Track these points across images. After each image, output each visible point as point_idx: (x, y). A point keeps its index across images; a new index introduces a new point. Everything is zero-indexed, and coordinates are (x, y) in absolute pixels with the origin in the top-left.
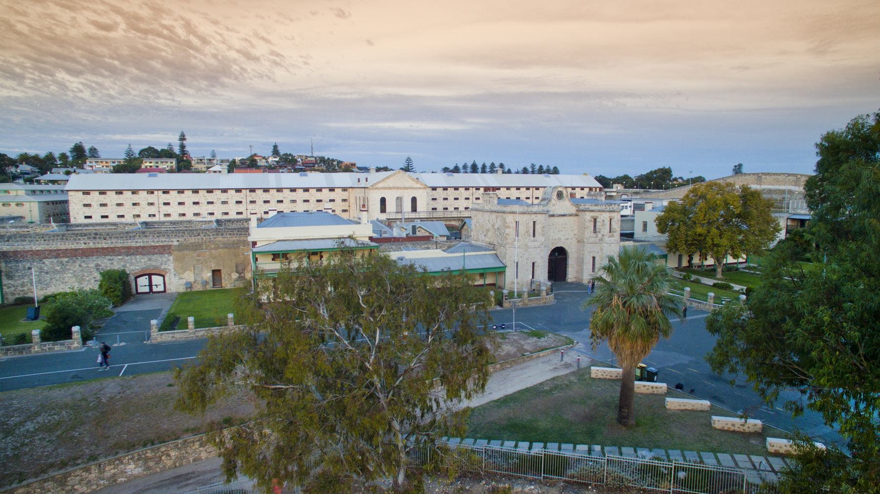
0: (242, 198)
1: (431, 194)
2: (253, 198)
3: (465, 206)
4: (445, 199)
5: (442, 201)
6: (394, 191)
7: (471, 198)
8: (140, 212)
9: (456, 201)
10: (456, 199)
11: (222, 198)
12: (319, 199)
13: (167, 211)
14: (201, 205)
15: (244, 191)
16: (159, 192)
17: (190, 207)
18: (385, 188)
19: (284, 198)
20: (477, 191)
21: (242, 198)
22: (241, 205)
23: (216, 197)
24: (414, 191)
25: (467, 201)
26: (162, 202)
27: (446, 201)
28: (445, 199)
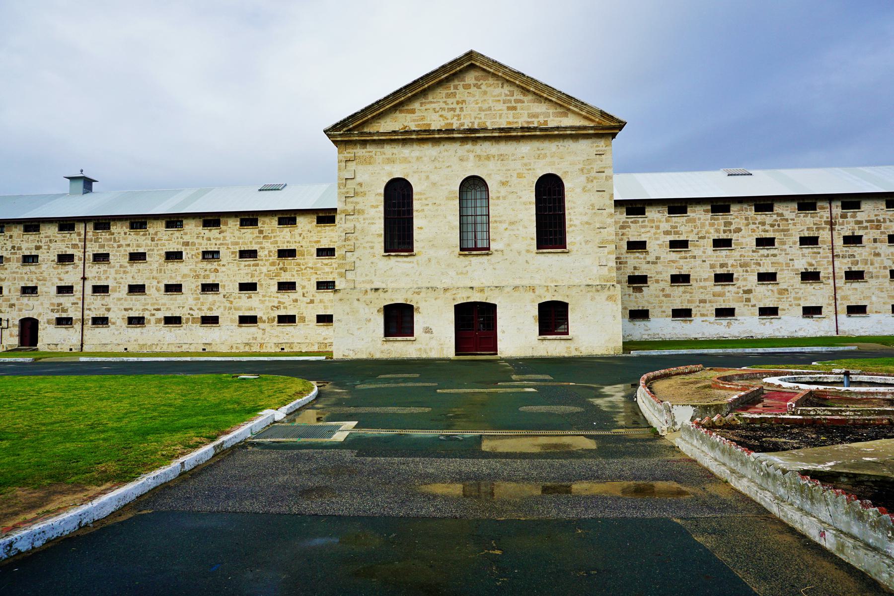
0: (75, 246)
1: (665, 226)
2: (102, 246)
3: (801, 265)
4: (721, 243)
5: (710, 248)
6: (450, 152)
7: (824, 235)
9: (764, 251)
10: (765, 242)
11: (24, 246)
12: (284, 247)
18: (405, 138)
19: (186, 244)
20: (850, 212)
21: (75, 246)
23: (9, 245)
24: (551, 147)
25: (808, 250)
27: (723, 253)
28: (721, 243)
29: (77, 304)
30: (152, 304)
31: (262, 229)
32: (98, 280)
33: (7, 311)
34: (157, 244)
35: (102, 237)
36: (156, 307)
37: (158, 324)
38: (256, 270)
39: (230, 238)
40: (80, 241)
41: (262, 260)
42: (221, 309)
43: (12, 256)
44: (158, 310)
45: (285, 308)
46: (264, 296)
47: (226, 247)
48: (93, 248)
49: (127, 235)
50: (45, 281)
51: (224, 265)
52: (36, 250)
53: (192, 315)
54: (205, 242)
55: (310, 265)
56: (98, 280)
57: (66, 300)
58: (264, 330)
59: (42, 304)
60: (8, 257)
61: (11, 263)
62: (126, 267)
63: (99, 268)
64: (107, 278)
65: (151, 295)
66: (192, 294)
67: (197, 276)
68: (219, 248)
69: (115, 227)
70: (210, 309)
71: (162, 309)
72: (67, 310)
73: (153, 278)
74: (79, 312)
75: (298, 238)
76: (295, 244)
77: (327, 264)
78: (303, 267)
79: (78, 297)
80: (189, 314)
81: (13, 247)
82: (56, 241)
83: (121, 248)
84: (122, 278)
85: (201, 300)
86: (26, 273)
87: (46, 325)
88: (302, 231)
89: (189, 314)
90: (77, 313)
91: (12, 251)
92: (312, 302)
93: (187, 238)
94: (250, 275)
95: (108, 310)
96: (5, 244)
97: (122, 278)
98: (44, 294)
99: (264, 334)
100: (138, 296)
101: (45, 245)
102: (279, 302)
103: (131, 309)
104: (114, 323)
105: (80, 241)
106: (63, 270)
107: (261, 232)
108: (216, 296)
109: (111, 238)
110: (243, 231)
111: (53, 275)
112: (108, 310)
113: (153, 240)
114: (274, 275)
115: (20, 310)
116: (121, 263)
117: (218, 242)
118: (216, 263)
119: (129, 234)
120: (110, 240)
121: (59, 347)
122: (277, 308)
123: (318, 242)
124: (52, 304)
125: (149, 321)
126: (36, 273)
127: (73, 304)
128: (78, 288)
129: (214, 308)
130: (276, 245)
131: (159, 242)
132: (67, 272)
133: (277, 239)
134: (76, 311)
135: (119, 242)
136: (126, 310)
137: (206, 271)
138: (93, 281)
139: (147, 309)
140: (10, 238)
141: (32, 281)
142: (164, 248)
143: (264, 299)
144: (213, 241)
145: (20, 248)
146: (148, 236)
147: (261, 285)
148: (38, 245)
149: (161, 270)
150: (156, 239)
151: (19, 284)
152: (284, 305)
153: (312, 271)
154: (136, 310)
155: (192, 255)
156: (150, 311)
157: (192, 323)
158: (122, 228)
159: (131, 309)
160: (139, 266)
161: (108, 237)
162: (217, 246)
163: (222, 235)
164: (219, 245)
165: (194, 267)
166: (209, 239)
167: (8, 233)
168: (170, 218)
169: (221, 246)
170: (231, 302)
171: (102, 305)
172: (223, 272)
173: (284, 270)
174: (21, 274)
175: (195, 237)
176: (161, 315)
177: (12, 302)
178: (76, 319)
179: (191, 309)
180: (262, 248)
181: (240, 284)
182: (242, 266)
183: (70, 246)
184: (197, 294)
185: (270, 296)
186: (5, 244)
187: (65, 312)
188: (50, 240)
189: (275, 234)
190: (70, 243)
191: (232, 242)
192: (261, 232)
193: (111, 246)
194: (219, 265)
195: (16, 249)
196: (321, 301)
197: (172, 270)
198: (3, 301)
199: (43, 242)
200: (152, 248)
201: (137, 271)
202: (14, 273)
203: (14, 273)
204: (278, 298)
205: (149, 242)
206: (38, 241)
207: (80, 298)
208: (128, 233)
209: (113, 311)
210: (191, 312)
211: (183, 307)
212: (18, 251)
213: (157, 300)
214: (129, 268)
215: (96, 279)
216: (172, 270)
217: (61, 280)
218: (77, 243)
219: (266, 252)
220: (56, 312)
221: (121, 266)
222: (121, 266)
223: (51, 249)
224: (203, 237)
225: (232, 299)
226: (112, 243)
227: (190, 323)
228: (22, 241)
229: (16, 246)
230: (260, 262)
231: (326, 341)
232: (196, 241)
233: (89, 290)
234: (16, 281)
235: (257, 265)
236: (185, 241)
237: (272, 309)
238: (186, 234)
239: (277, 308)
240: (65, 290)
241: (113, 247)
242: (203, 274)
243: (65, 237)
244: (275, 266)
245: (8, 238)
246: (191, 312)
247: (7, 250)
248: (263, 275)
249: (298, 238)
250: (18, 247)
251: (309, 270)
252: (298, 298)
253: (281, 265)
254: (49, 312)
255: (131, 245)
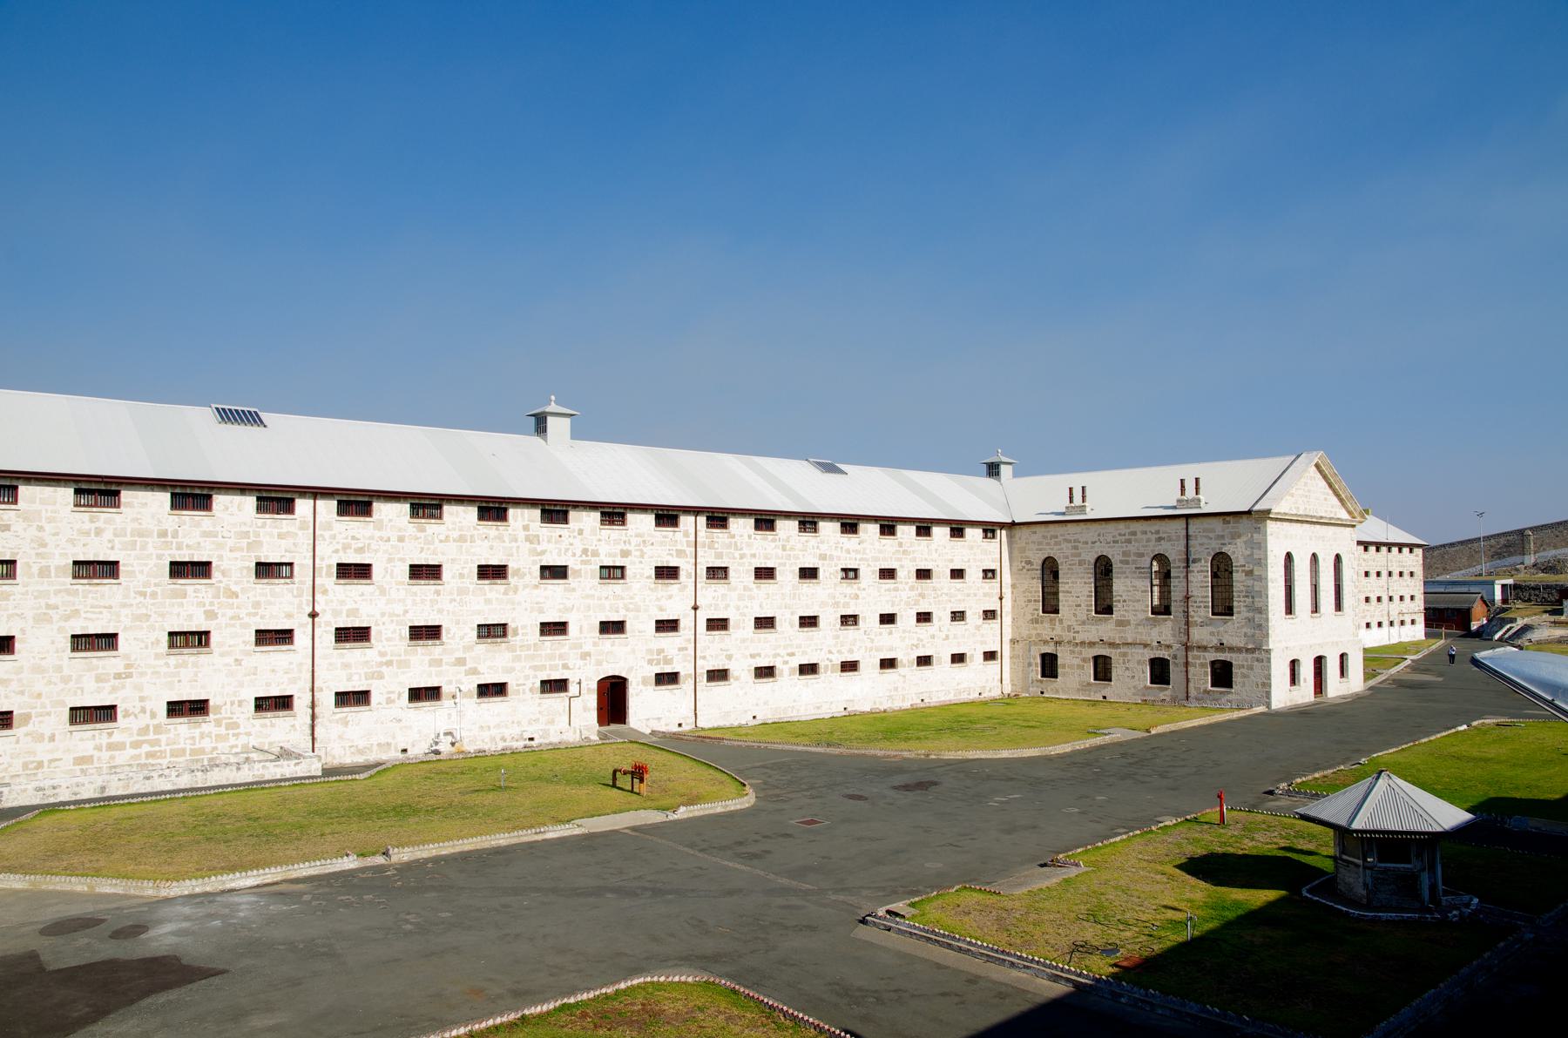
0: (680, 553)
2: (719, 556)
8: (210, 615)
13: (353, 612)
14: (511, 579)
15: (686, 521)
16: (321, 504)
17: (462, 591)
19: (823, 557)
21: (680, 553)
22: (672, 587)
26: (330, 558)
29: (686, 649)
30: (785, 647)
31: (901, 540)
32: (715, 610)
33: (577, 666)
34: (790, 555)
35: (720, 540)
36: (790, 651)
37: (792, 677)
38: (896, 597)
39: (871, 551)
40: (688, 546)
41: (901, 583)
42: (863, 651)
43: (583, 566)
44: (792, 654)
45: (924, 646)
46: (904, 631)
47: (866, 563)
48: (708, 559)
49: (752, 540)
50: (639, 611)
51: (864, 589)
52: (622, 557)
53: (831, 661)
54: (844, 554)
55: (945, 591)
56: (715, 610)
57: (668, 640)
58: (904, 676)
59: (633, 651)
60: (577, 568)
61: (582, 579)
62: (750, 590)
63: (715, 591)
64: (727, 606)
65: (783, 632)
66: (831, 630)
67: (837, 604)
68: (859, 565)
69: (735, 526)
70: (851, 651)
71: (797, 654)
72: (672, 659)
73: (786, 608)
74: (690, 662)
75: (935, 556)
76: (931, 563)
77: (959, 590)
78: (939, 593)
79: (688, 637)
80: (828, 659)
81: (585, 551)
82: (652, 544)
83: (744, 560)
84: (747, 607)
85: (841, 639)
86: (607, 598)
87: (641, 687)
88: (939, 546)
89: (828, 659)
90: (686, 664)
91: (584, 557)
92: (947, 637)
93: (824, 547)
94: (890, 603)
95: (729, 657)
96: (571, 544)
97: (747, 607)
98: (638, 634)
99: (904, 682)
100: (767, 635)
101: (637, 550)
102: (918, 639)
103: (759, 655)
104: (737, 679)
105: (688, 546)
106: (664, 594)
107: (900, 545)
108: (857, 632)
109: (730, 542)
110: (884, 541)
111: (650, 601)
112: (729, 657)
113: (784, 550)
114: (913, 603)
115: (599, 663)
116: (745, 584)
117: (858, 556)
118: (855, 586)
119: (755, 538)
120: (729, 546)
121: (663, 722)
122: (917, 646)
123: (952, 561)
124: (650, 651)
125: (781, 675)
126: (622, 598)
127: (680, 649)
128: (686, 624)
129: (855, 650)
130: (914, 564)
131: (791, 553)
132: (670, 597)
133: (915, 555)
134: (685, 661)
135: (741, 549)
136: (752, 656)
137: (845, 596)
138: (708, 611)
139: (779, 655)
140: (579, 534)
141: (617, 612)
142: (798, 561)
143: (903, 635)
144: (853, 555)
145: (595, 554)
146: (777, 543)
147: (902, 616)
148: (625, 548)
149: (795, 594)
150: (788, 547)
151: (596, 617)
152: (924, 643)
153: (947, 598)
154: (765, 656)
155: (830, 574)
156: (783, 657)
157: (832, 672)
158: (745, 527)
159: (759, 655)
160: (766, 586)
161: (727, 541)
162: (857, 562)
163: (862, 546)
164: (860, 560)
165: (831, 591)
166: (848, 551)
167: (577, 524)
168: (804, 517)
169: (861, 563)
170: (872, 641)
171: (721, 650)
172: (864, 598)
173: (922, 596)
174: (599, 599)
175: (833, 548)
176: (796, 663)
177: (586, 648)
178: (685, 675)
179: (830, 652)
180: (902, 566)
181: (881, 616)
182: (883, 590)
183: (675, 554)
184: (836, 630)
185: (910, 632)
186: (571, 544)
187: (670, 664)
188: (644, 542)
189: (913, 549)
190: (674, 548)
191: (872, 557)
192: (900, 545)
193: (731, 556)
194: (859, 589)
195: (589, 553)
196: (955, 637)
197: (807, 596)
198: (570, 648)
199: (633, 544)
200: (783, 561)
201: (766, 597)
202: (588, 596)
203: (588, 596)
204: (916, 633)
205: (780, 552)
206: (625, 542)
207: (689, 640)
208: (753, 536)
209: (736, 659)
210: (830, 656)
211: (821, 649)
212: (592, 559)
213: (791, 640)
214: (755, 590)
215: (712, 608)
216: (807, 596)
217: (661, 609)
218: (685, 548)
219: (906, 573)
220: (656, 664)
221: (746, 588)
222: (746, 588)
223: (646, 556)
224: (842, 548)
225: (873, 637)
226: (732, 551)
227: (829, 672)
228: (600, 540)
229: (590, 548)
230: (900, 586)
231: (959, 687)
232: (835, 553)
233: (702, 625)
234: (591, 613)
235: (896, 590)
236: (822, 552)
237: (912, 649)
238: (822, 542)
239: (917, 646)
240: (667, 626)
241: (734, 558)
242: (842, 601)
243: (665, 537)
244: (913, 590)
245: (576, 534)
246: (830, 656)
247: (574, 555)
248: (903, 603)
249: (935, 556)
250: (592, 550)
251: (945, 598)
252: (935, 633)
253: (920, 591)
254: (645, 664)
255: (757, 555)
